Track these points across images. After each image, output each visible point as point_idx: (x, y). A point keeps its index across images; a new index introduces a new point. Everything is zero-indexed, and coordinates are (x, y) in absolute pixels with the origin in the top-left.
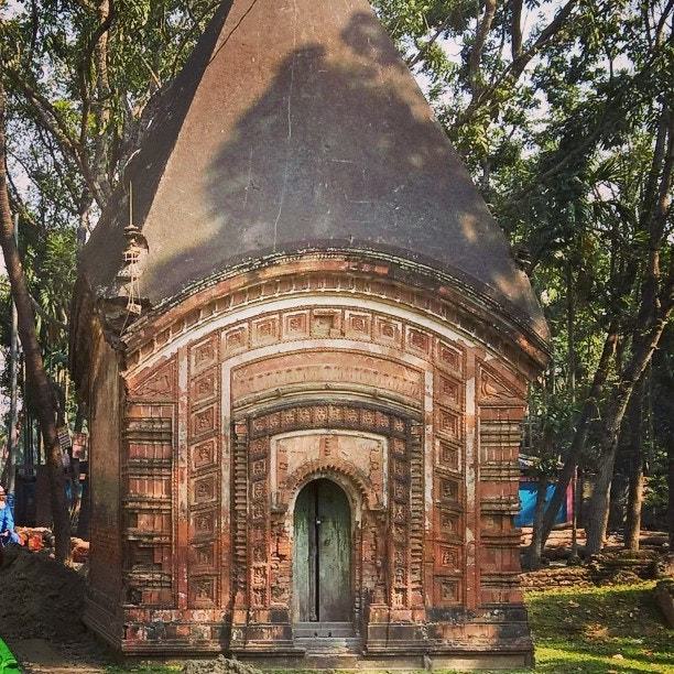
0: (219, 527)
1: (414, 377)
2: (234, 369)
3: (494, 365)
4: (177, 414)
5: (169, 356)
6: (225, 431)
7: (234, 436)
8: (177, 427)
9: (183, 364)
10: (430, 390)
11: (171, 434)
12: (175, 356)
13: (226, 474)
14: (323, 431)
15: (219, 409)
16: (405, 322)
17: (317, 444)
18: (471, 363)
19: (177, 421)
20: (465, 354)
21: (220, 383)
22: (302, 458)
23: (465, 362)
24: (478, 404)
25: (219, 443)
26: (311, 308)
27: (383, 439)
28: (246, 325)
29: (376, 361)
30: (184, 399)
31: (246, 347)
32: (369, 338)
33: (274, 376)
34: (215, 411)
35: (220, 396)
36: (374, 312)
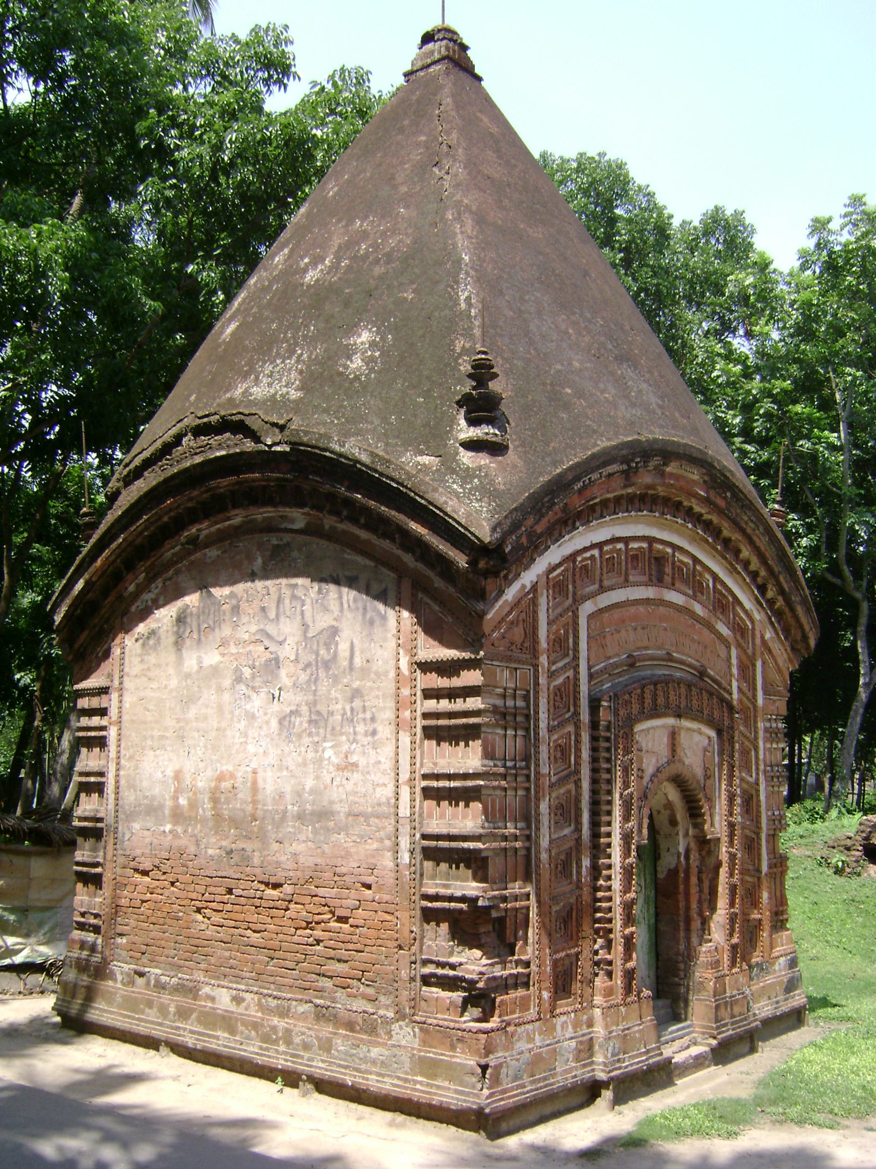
0: (579, 873)
1: (722, 651)
2: (590, 617)
3: (771, 645)
4: (537, 684)
5: (529, 587)
6: (585, 716)
7: (594, 725)
8: (537, 705)
9: (543, 601)
10: (735, 671)
11: (527, 717)
12: (534, 588)
13: (586, 785)
14: (670, 721)
15: (576, 679)
16: (716, 578)
17: (665, 740)
18: (758, 641)
19: (536, 698)
20: (753, 629)
21: (576, 637)
22: (654, 760)
23: (753, 639)
24: (766, 692)
25: (578, 735)
26: (651, 540)
27: (713, 734)
28: (596, 552)
29: (698, 626)
30: (543, 660)
31: (597, 586)
32: (690, 592)
33: (623, 633)
34: (572, 682)
35: (576, 658)
36: (696, 560)
